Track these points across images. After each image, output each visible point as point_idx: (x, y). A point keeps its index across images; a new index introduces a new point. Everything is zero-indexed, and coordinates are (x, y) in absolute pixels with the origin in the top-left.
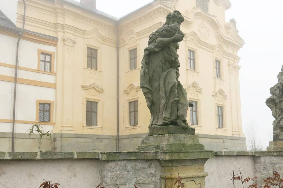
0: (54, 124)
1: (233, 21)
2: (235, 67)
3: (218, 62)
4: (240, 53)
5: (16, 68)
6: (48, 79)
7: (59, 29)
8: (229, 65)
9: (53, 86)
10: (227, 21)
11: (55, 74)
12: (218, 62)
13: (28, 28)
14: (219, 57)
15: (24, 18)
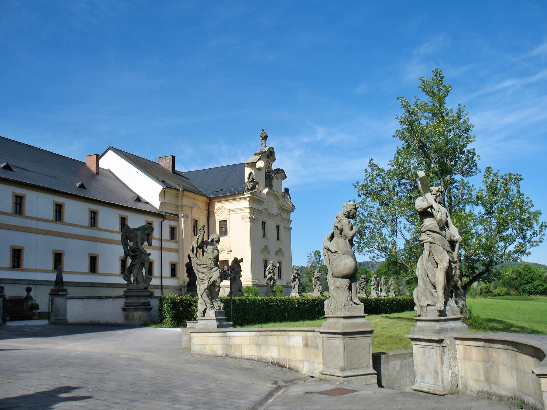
0: (178, 278)
1: (287, 190)
2: (288, 229)
3: (278, 227)
4: (292, 216)
5: (161, 240)
6: (173, 245)
7: (180, 209)
8: (285, 228)
9: (177, 251)
10: (283, 191)
11: (177, 242)
12: (278, 227)
13: (166, 211)
14: (279, 223)
15: (163, 204)
